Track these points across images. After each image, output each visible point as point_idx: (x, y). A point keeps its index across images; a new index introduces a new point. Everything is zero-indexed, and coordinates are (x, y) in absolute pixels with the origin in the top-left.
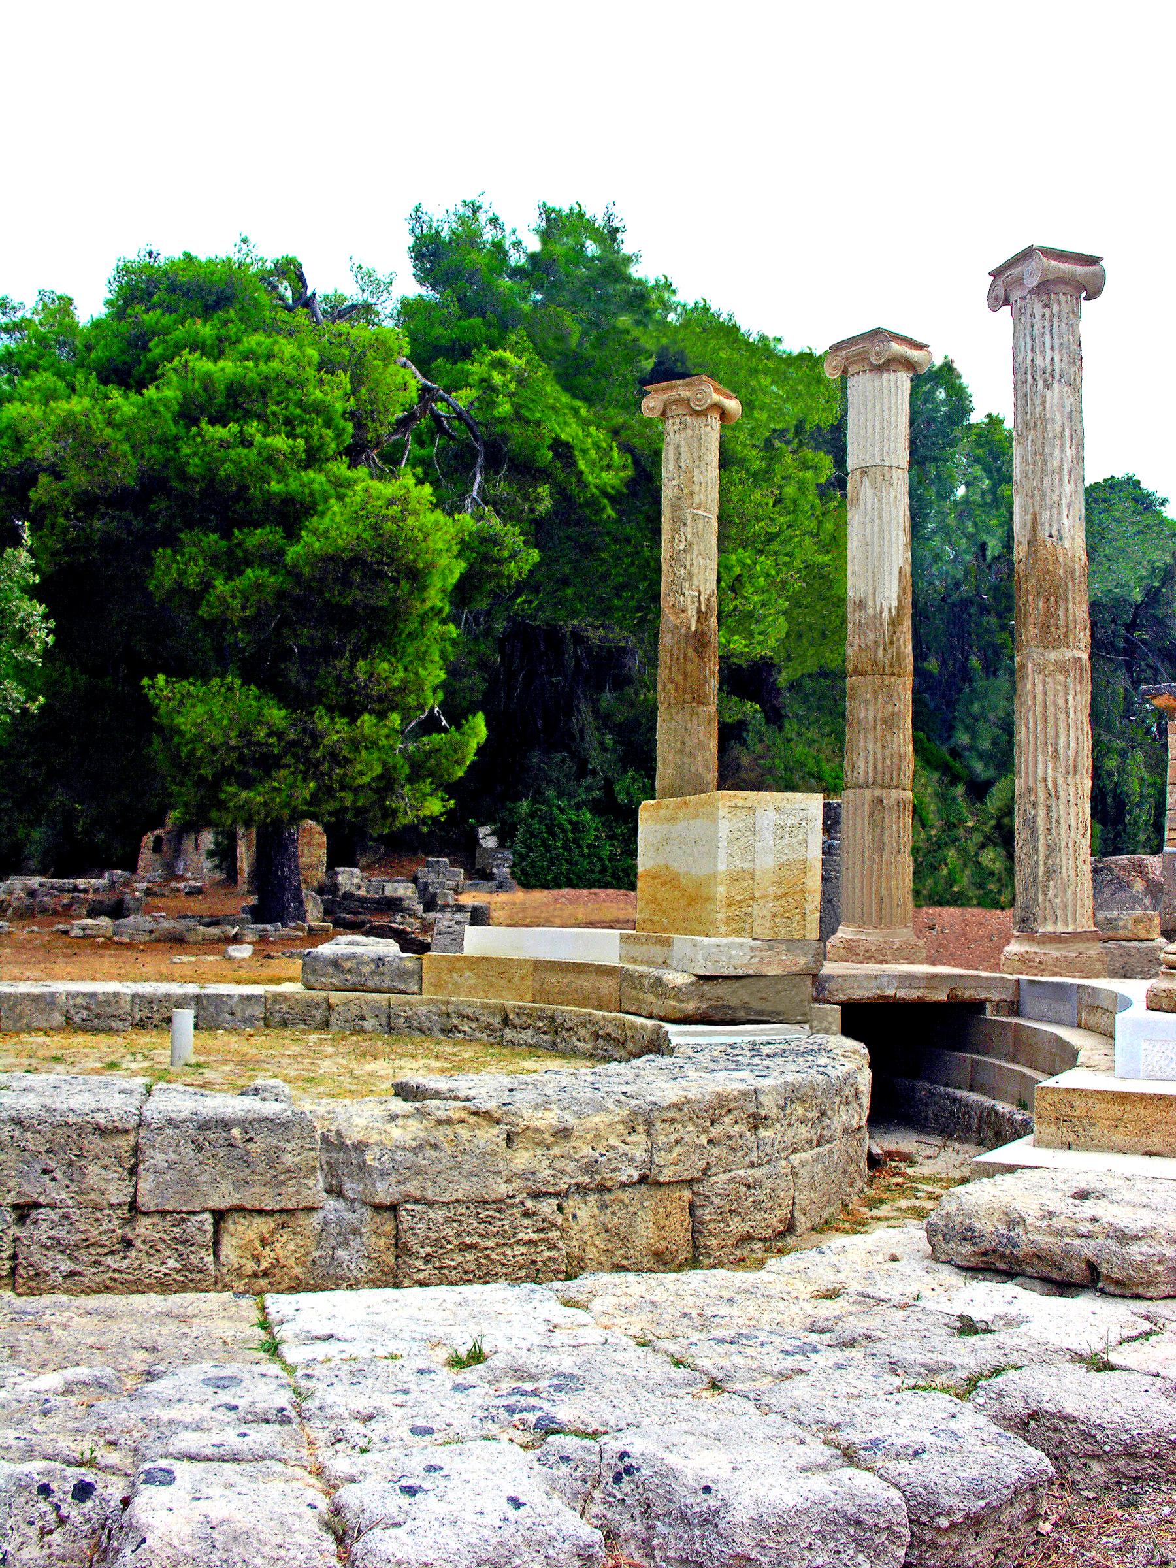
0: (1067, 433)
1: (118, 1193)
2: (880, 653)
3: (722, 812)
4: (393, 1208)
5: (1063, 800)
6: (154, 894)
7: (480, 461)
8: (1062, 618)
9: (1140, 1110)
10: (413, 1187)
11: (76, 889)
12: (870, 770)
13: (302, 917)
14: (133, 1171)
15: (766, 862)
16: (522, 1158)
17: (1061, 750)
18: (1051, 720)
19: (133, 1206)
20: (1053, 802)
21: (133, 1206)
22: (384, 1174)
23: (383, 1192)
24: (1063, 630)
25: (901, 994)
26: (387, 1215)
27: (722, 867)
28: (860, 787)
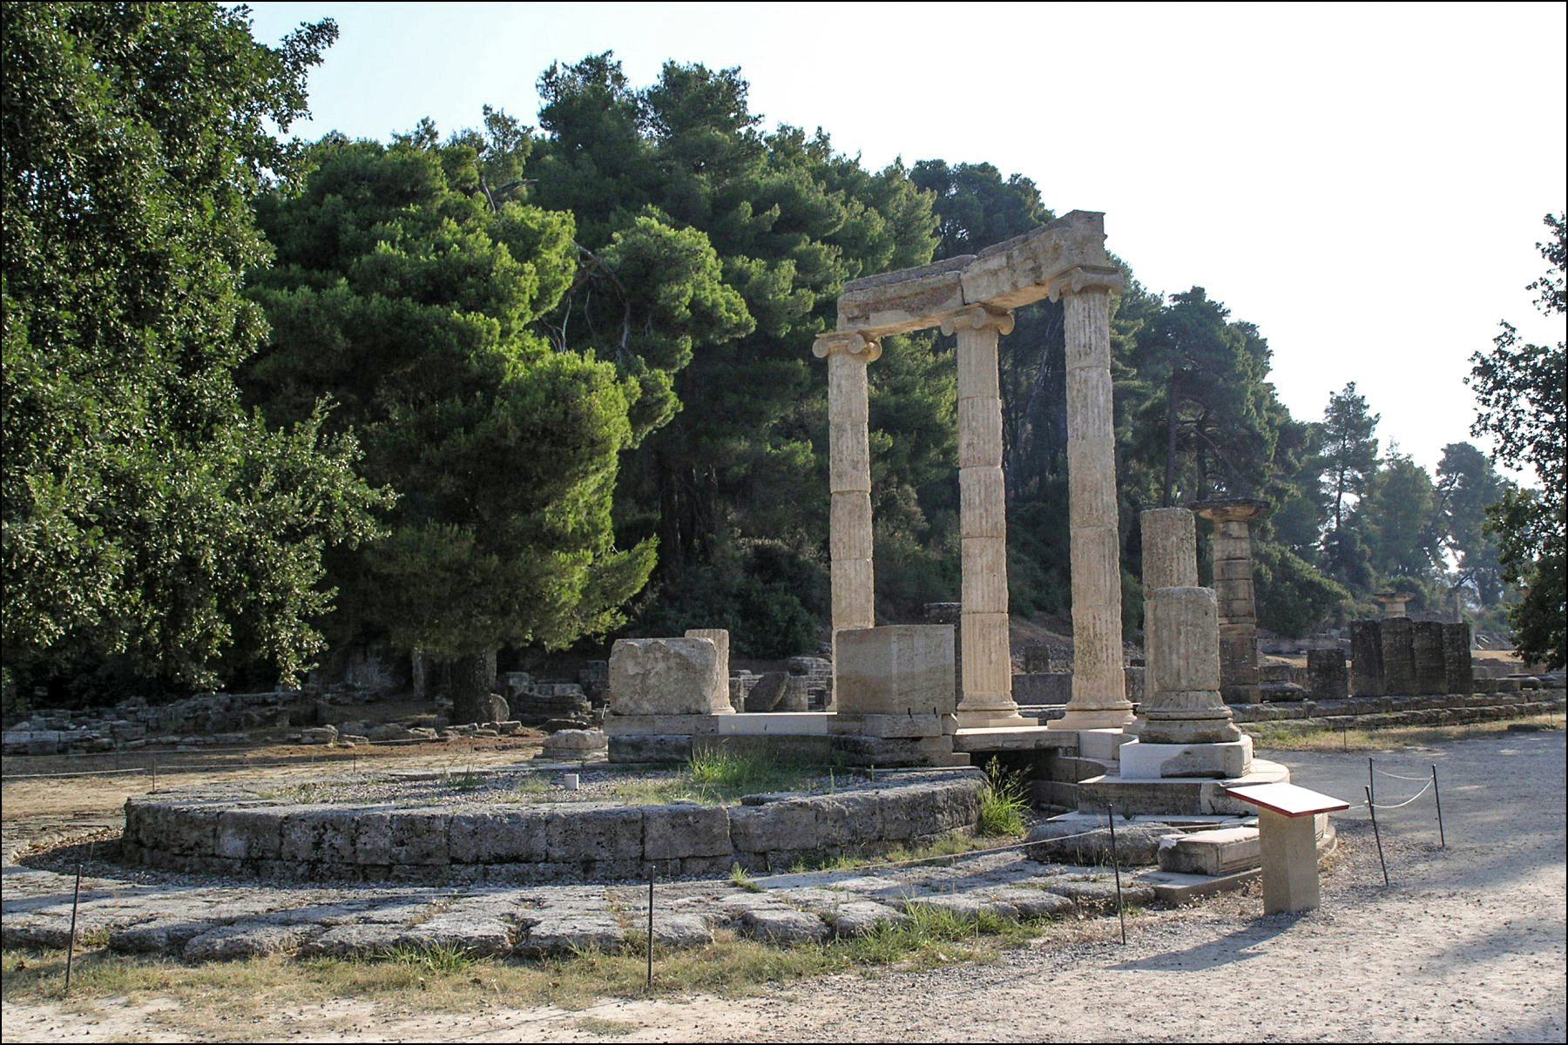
1: (635, 850)
3: (894, 638)
4: (764, 854)
6: (338, 703)
7: (628, 314)
9: (1131, 792)
10: (773, 843)
11: (265, 703)
13: (491, 718)
14: (642, 842)
15: (920, 667)
16: (822, 830)
19: (642, 858)
21: (642, 858)
22: (759, 837)
23: (759, 845)
26: (760, 858)
27: (895, 672)
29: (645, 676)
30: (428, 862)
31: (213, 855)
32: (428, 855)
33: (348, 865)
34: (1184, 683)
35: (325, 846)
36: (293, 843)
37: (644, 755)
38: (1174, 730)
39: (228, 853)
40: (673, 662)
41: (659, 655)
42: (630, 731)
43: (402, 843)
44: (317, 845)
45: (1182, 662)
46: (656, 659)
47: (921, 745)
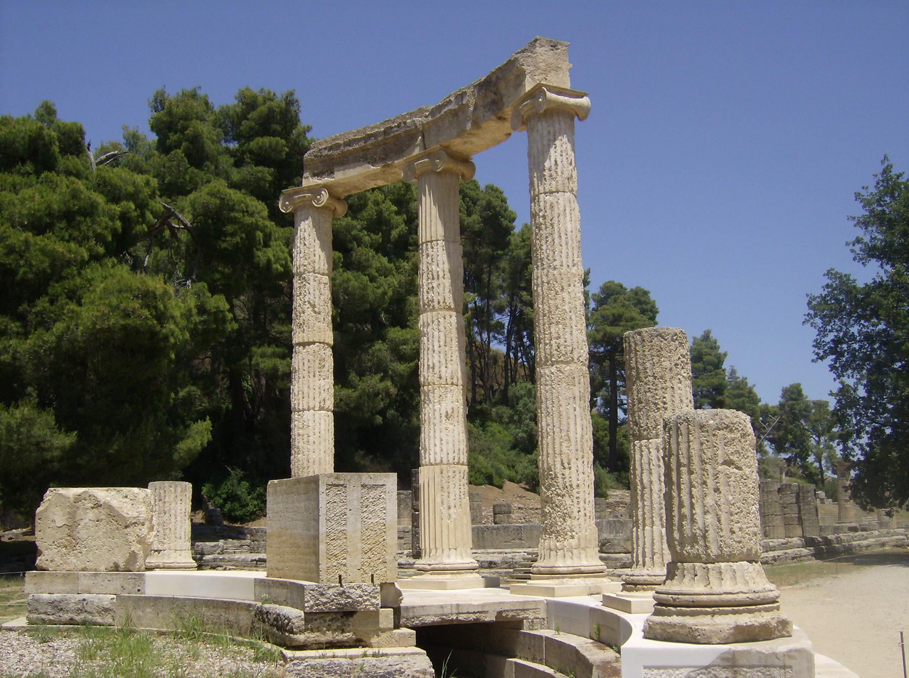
0: (568, 211)
2: (443, 369)
5: (574, 469)
8: (569, 340)
12: (438, 449)
17: (572, 434)
18: (564, 414)
20: (567, 472)
24: (570, 348)
25: (462, 617)
28: (431, 464)
37: (66, 616)
38: (702, 622)
40: (102, 513)
45: (710, 519)
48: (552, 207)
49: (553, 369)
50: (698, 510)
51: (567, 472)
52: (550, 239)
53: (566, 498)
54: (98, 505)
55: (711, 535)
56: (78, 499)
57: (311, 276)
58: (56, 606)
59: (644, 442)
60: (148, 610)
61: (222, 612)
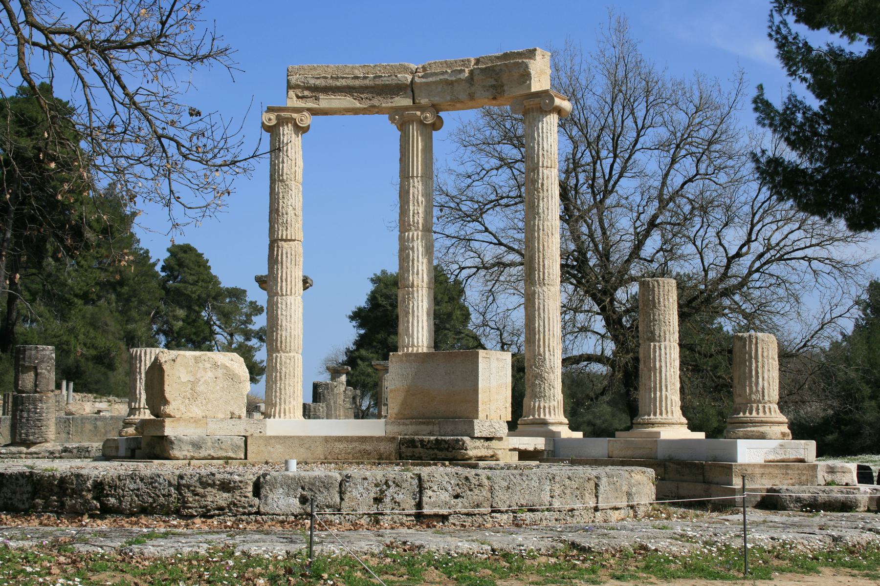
21: (596, 509)
29: (194, 384)
30: (476, 511)
31: (258, 513)
32: (478, 506)
33: (407, 515)
34: (766, 398)
35: (387, 500)
36: (351, 499)
37: (203, 453)
39: (278, 511)
40: (220, 373)
41: (208, 365)
42: (187, 432)
43: (457, 497)
44: (378, 500)
46: (205, 369)
47: (494, 443)
48: (547, 178)
49: (545, 289)
50: (760, 380)
51: (552, 358)
52: (545, 200)
53: (551, 375)
54: (216, 365)
55: (766, 391)
56: (196, 358)
57: (293, 184)
58: (196, 445)
59: (657, 344)
60: (278, 446)
61: (354, 444)
